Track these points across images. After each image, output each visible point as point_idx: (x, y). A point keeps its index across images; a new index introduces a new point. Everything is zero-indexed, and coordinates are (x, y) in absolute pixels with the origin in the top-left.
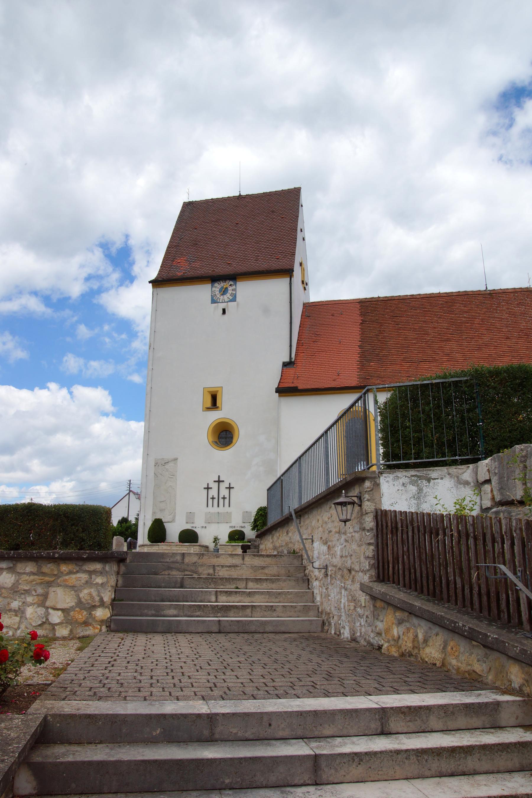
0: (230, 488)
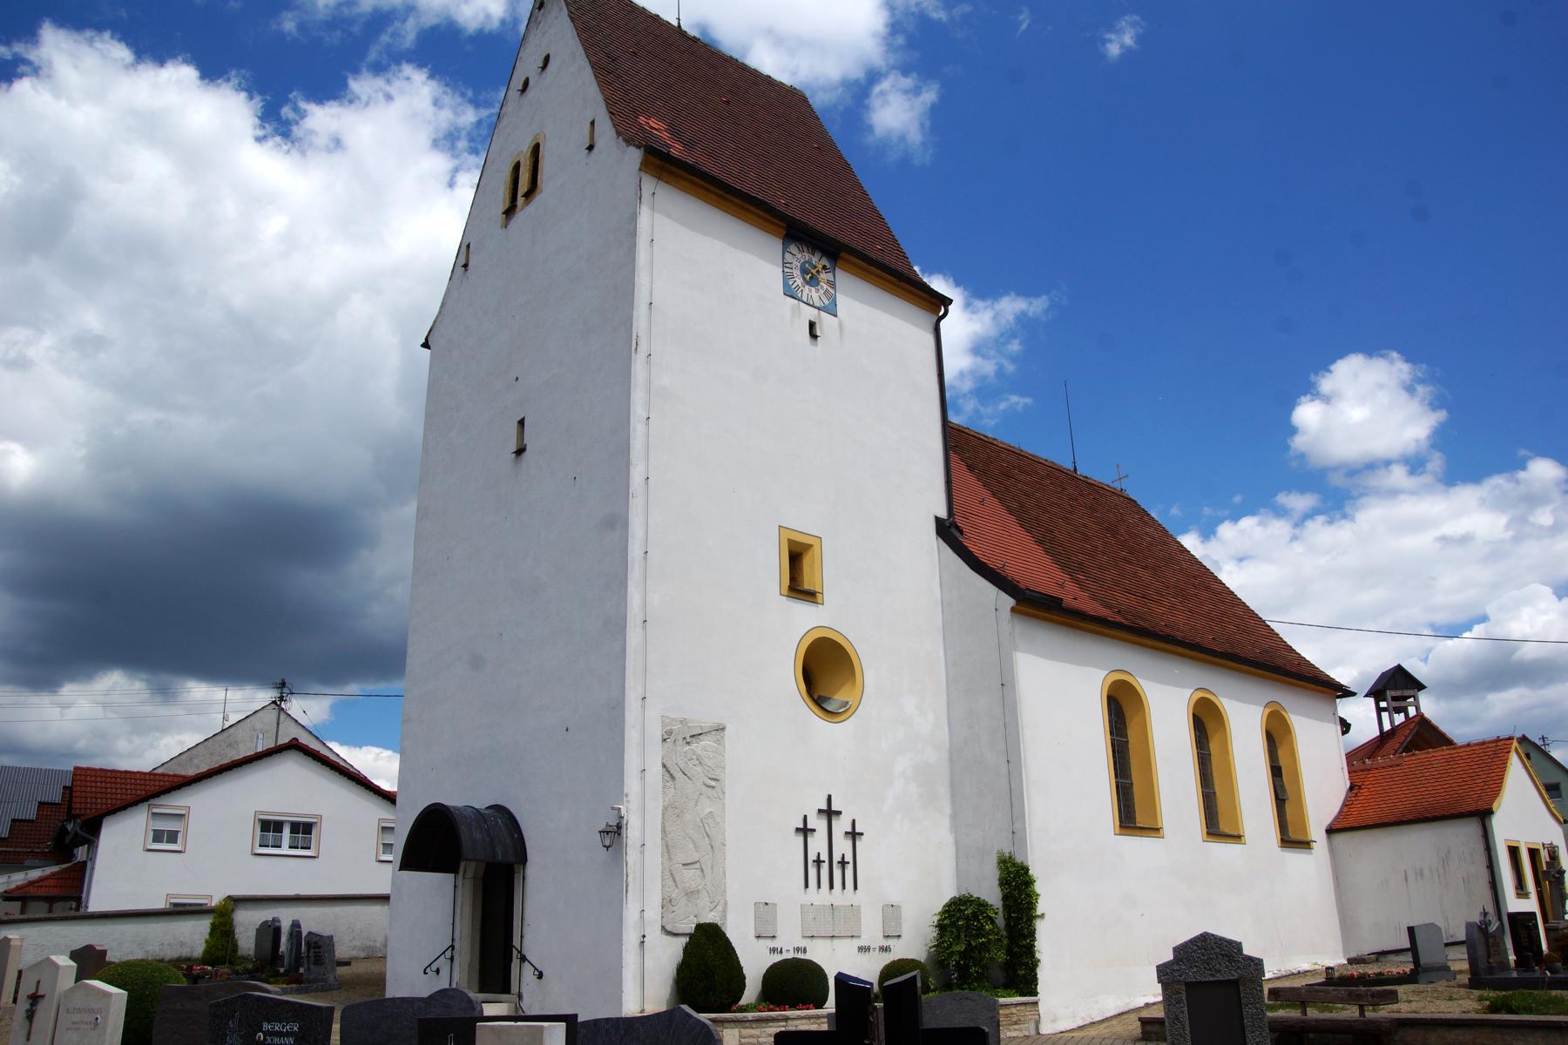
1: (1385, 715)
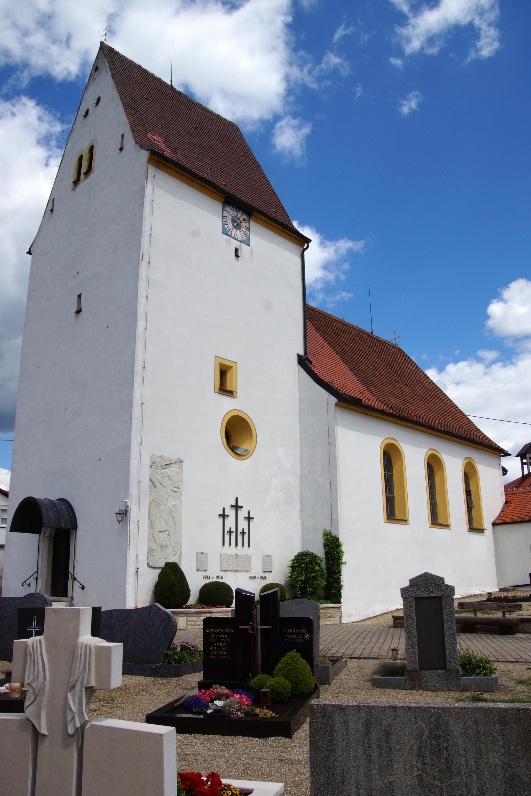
0: (249, 519)
1: (525, 466)
